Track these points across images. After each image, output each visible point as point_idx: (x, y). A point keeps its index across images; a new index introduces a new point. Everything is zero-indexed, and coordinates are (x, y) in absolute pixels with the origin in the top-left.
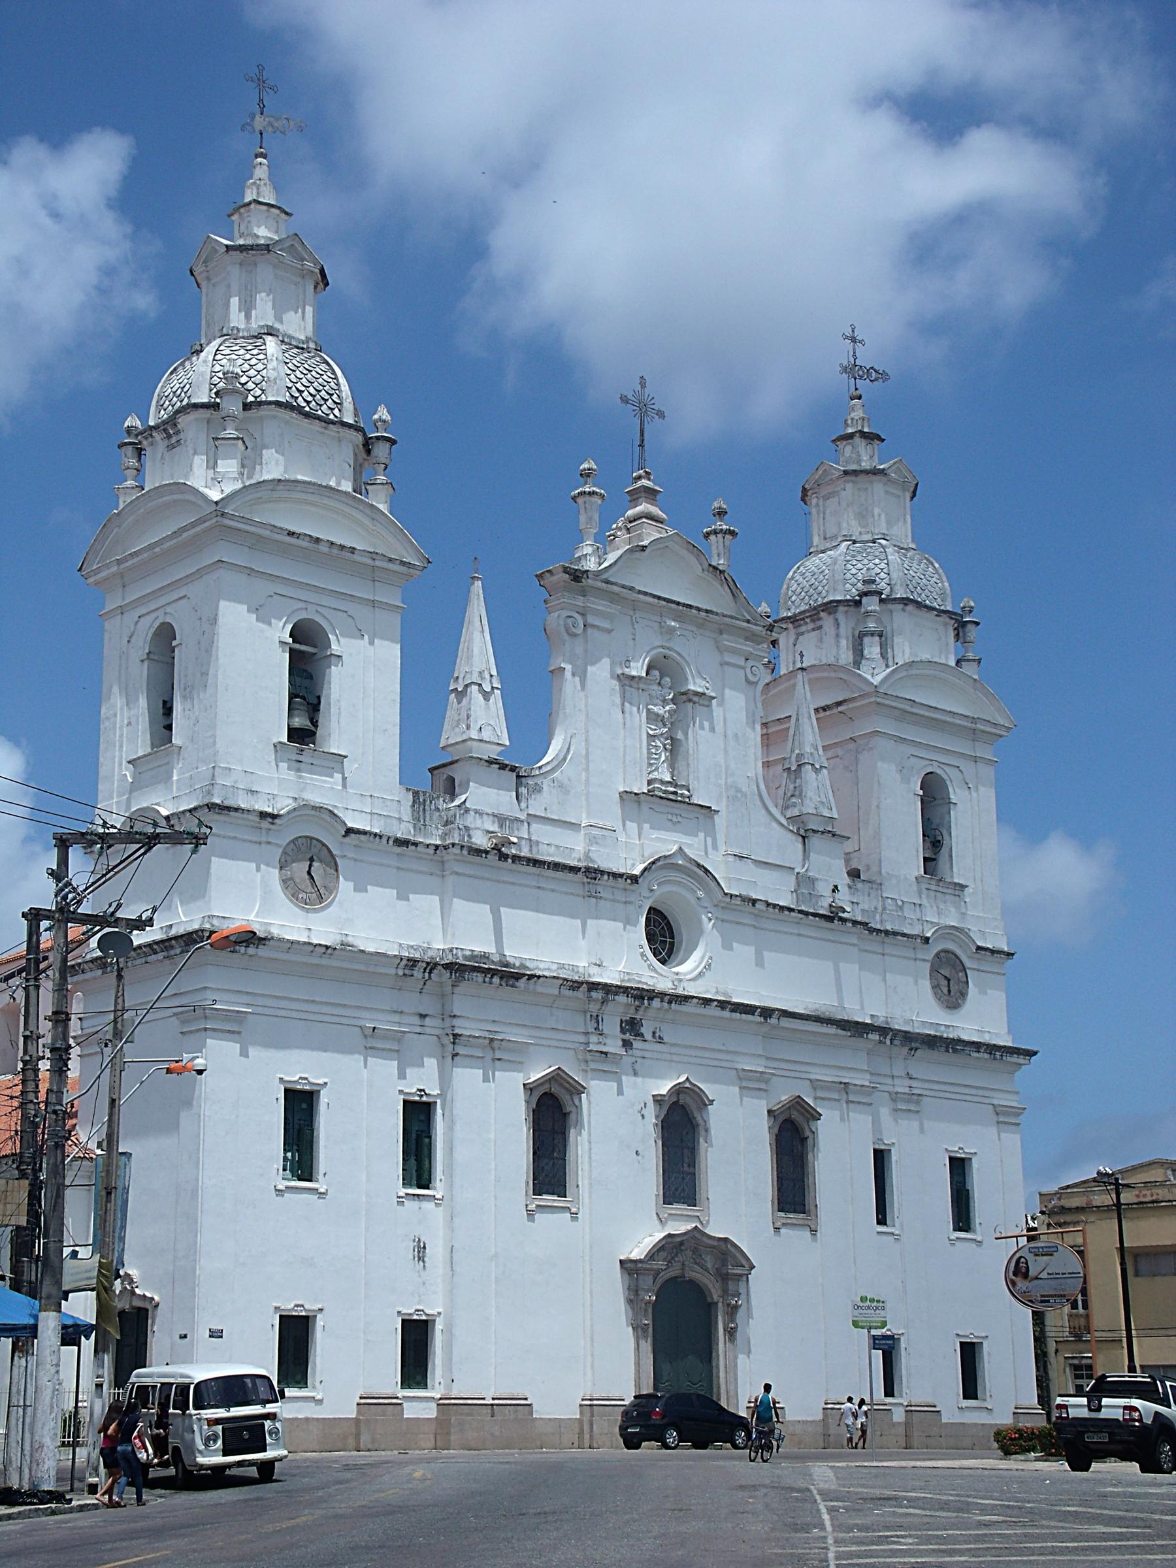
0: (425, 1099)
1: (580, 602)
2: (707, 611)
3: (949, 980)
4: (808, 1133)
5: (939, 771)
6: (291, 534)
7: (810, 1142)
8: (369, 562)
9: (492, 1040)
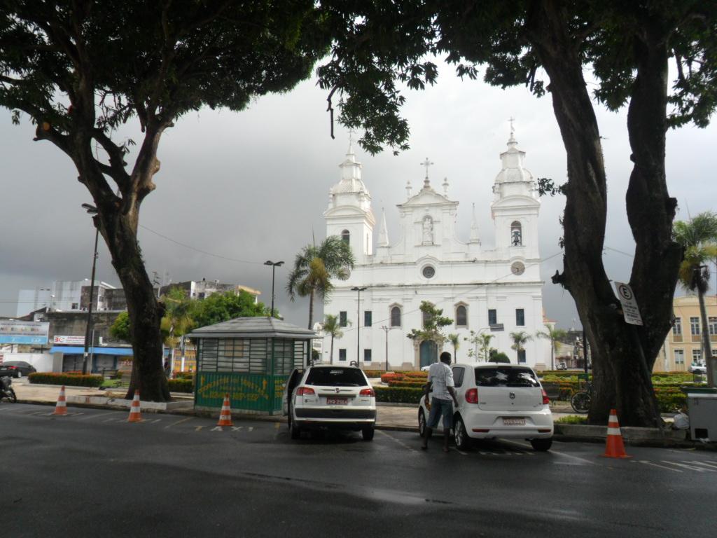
1: (403, 210)
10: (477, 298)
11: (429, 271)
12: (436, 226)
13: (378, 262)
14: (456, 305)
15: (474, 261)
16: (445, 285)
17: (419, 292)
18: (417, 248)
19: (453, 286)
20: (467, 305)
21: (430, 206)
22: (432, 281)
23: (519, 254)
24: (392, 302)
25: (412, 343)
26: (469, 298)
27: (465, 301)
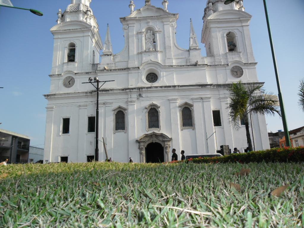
0: (92, 116)
1: (126, 23)
2: (157, 16)
3: (237, 72)
4: (191, 109)
5: (231, 31)
6: (65, 30)
7: (192, 111)
8: (80, 30)
9: (104, 103)
10: (202, 98)
11: (152, 77)
12: (158, 36)
13: (102, 68)
14: (180, 107)
15: (196, 65)
16: (170, 87)
17: (144, 95)
18: (140, 55)
19: (177, 88)
20: (192, 106)
21: (151, 18)
22: (155, 84)
23: (238, 59)
24: (115, 106)
25: (138, 147)
26: (192, 99)
27: (190, 102)
